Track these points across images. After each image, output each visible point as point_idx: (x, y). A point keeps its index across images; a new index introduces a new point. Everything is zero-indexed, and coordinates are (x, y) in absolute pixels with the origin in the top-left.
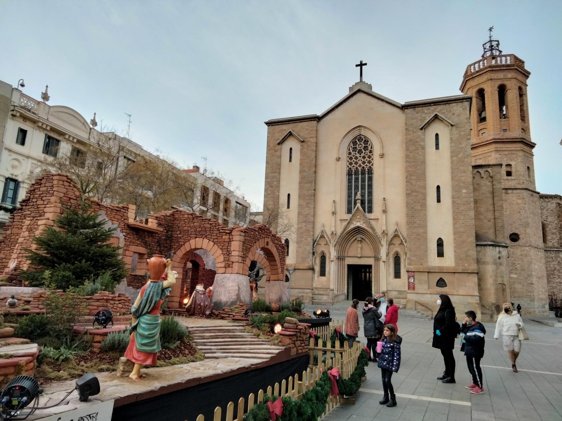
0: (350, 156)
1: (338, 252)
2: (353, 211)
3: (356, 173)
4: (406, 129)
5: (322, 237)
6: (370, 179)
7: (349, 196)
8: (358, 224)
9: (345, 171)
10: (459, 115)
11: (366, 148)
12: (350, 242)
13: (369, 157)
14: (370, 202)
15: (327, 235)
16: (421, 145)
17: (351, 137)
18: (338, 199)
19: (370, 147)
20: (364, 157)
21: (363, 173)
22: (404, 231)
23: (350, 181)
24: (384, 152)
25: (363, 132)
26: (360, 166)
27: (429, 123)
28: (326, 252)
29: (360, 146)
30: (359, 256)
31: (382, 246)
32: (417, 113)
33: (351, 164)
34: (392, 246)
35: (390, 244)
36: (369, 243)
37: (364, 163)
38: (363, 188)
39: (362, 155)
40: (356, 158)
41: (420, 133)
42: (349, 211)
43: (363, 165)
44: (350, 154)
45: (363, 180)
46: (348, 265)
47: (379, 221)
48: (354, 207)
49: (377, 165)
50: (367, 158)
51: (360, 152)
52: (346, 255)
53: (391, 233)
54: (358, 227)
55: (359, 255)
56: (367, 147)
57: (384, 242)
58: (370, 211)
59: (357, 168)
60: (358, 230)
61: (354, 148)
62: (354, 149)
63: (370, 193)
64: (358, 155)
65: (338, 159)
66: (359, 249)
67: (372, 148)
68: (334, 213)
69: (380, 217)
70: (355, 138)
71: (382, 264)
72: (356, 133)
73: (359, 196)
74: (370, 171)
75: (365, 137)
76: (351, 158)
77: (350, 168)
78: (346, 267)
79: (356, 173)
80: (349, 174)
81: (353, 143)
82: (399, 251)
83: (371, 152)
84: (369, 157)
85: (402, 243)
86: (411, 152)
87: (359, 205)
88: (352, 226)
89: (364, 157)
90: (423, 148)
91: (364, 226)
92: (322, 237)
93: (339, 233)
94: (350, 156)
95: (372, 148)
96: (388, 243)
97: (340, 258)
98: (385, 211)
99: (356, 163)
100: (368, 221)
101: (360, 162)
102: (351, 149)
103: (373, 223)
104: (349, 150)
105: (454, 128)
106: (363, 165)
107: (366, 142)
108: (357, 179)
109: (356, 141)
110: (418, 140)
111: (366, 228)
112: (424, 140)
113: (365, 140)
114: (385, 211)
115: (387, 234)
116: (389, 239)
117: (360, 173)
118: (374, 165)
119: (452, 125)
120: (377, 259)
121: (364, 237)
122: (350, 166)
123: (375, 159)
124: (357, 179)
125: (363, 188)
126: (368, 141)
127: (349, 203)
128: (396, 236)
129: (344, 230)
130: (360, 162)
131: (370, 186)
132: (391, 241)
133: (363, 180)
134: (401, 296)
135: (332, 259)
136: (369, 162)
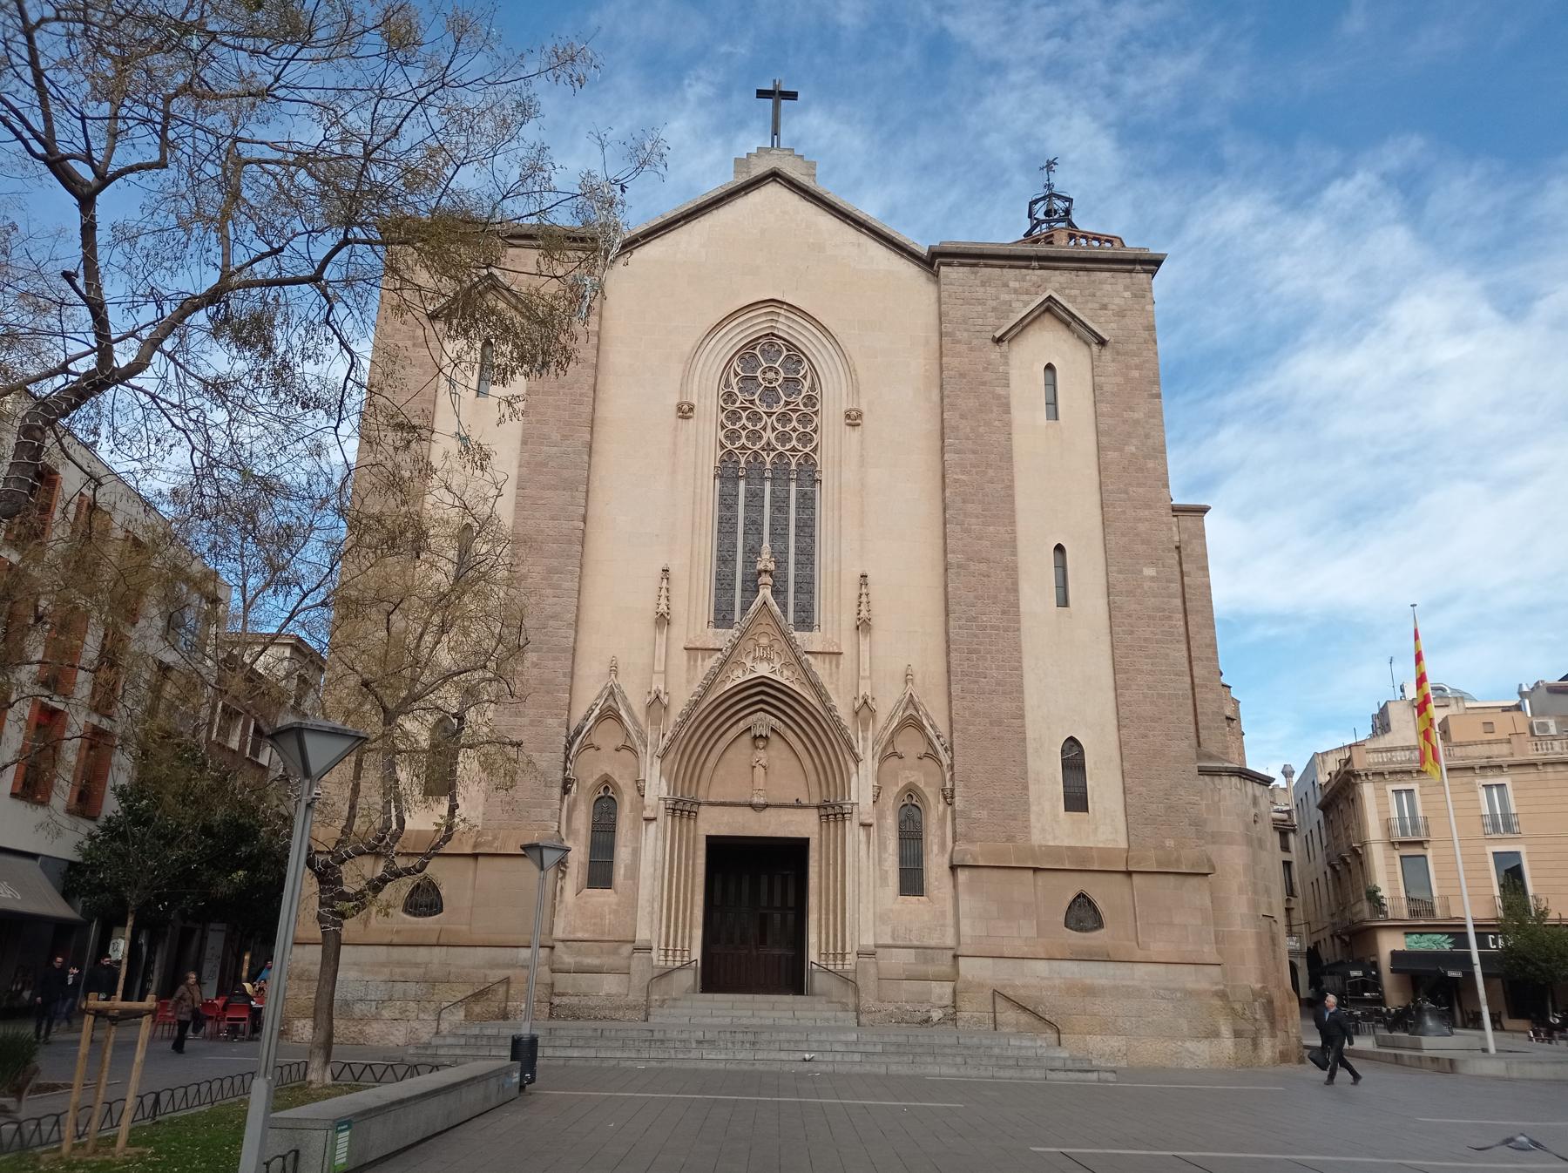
1: (673, 779)
3: (755, 471)
7: (725, 558)
8: (763, 670)
10: (1121, 314)
11: (792, 383)
14: (806, 586)
16: (999, 397)
17: (735, 337)
19: (807, 384)
22: (935, 712)
23: (726, 503)
25: (785, 326)
27: (1023, 325)
29: (771, 375)
31: (857, 760)
32: (983, 284)
33: (732, 436)
34: (894, 761)
35: (889, 753)
38: (779, 533)
39: (778, 409)
40: (755, 417)
41: (995, 353)
42: (722, 618)
44: (730, 398)
45: (780, 505)
46: (708, 837)
47: (846, 662)
51: (770, 394)
53: (887, 707)
54: (763, 682)
55: (760, 793)
57: (866, 747)
58: (806, 620)
60: (763, 693)
61: (744, 379)
62: (748, 381)
63: (807, 556)
67: (813, 388)
70: (752, 344)
71: (853, 832)
72: (758, 324)
73: (765, 561)
74: (809, 474)
75: (790, 346)
76: (734, 416)
79: (755, 471)
80: (727, 474)
83: (810, 400)
84: (805, 419)
86: (963, 417)
87: (765, 592)
88: (739, 677)
89: (784, 418)
91: (785, 677)
94: (730, 408)
96: (879, 749)
98: (863, 626)
99: (755, 436)
100: (797, 660)
102: (734, 381)
103: (819, 667)
104: (728, 384)
105: (1107, 354)
107: (796, 356)
108: (754, 498)
110: (988, 376)
114: (863, 626)
119: (1102, 342)
120: (833, 812)
124: (754, 498)
125: (779, 533)
127: (723, 584)
128: (913, 722)
129: (707, 689)
130: (769, 435)
131: (807, 528)
132: (891, 741)
133: (780, 505)
134: (931, 969)
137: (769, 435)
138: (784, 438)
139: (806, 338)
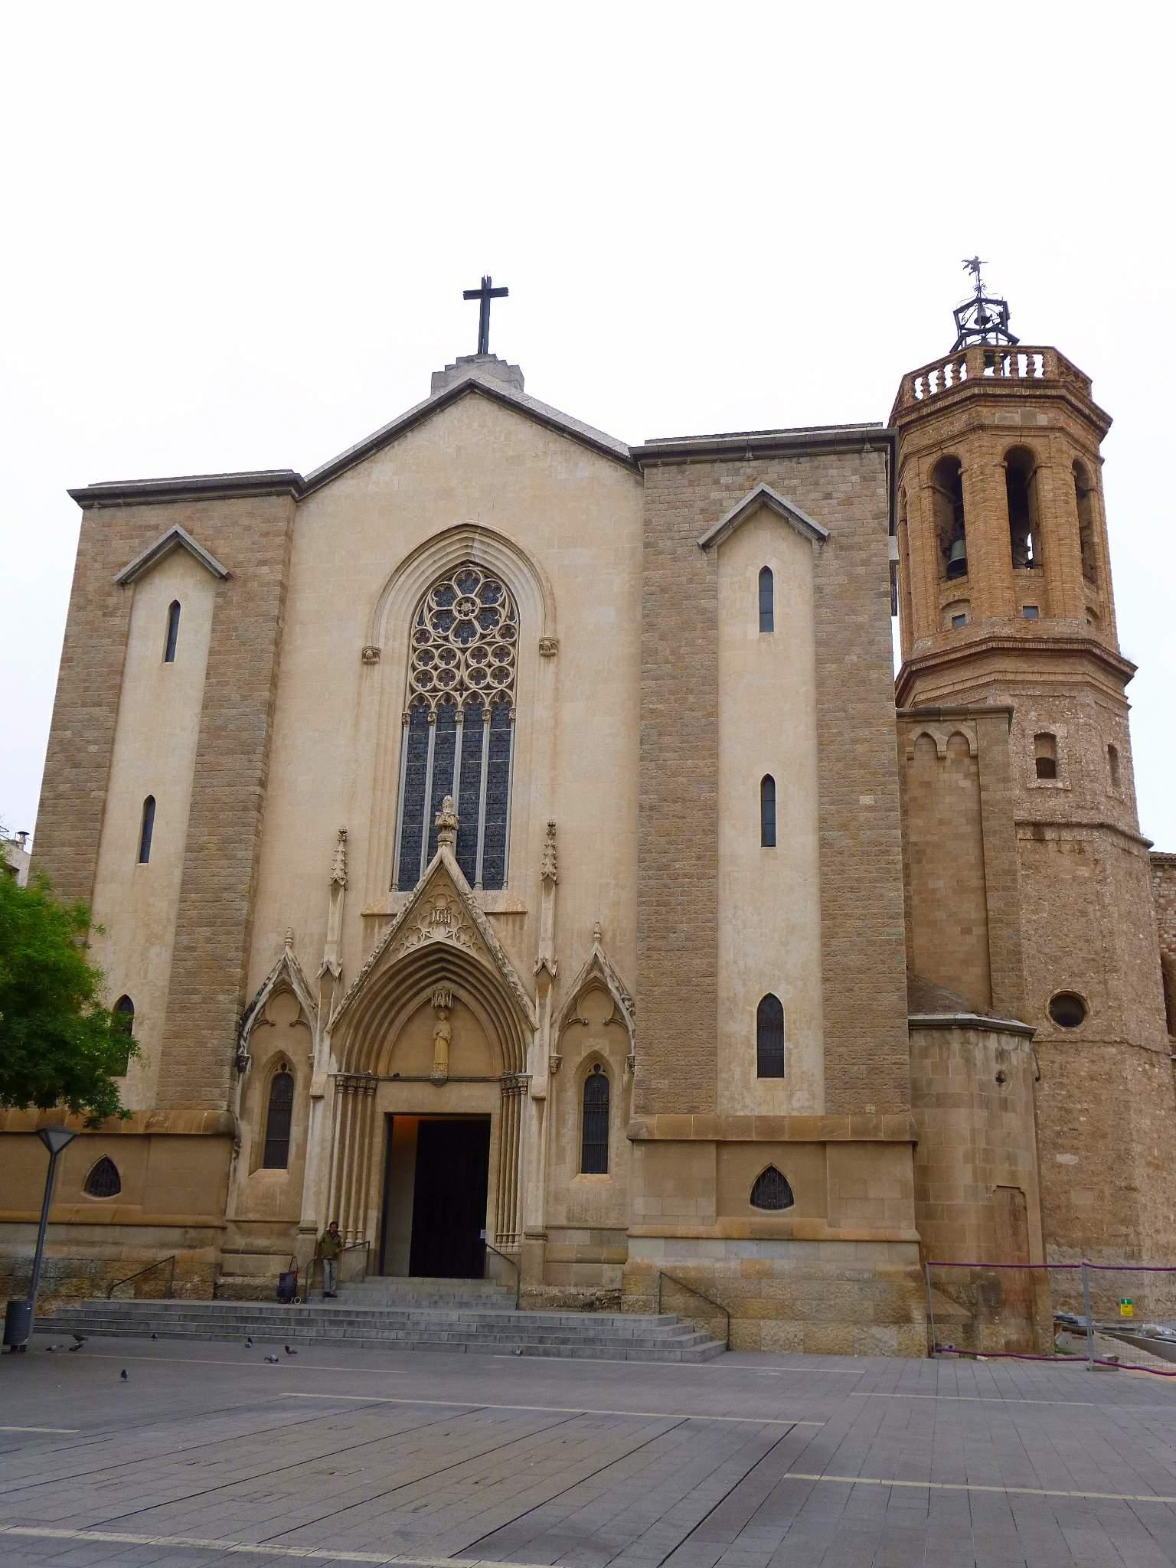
0: (423, 646)
4: (647, 545)
5: (283, 989)
6: (501, 744)
7: (412, 812)
8: (439, 935)
11: (488, 616)
14: (497, 840)
16: (703, 611)
18: (358, 825)
19: (504, 613)
20: (479, 654)
21: (473, 720)
24: (561, 636)
25: (479, 551)
26: (462, 687)
28: (296, 1058)
29: (467, 606)
30: (437, 1075)
38: (470, 781)
39: (473, 643)
41: (701, 562)
44: (423, 636)
47: (527, 920)
48: (429, 861)
49: (533, 685)
50: (490, 658)
51: (464, 630)
55: (438, 1071)
56: (494, 611)
58: (494, 879)
59: (448, 697)
60: (439, 961)
62: (442, 618)
63: (498, 804)
64: (455, 644)
65: (370, 657)
66: (441, 1045)
67: (511, 617)
69: (530, 908)
70: (448, 575)
72: (453, 553)
75: (488, 572)
76: (426, 657)
77: (421, 698)
78: (380, 1122)
80: (416, 718)
81: (437, 593)
82: (606, 1053)
83: (508, 632)
84: (501, 653)
85: (616, 1020)
87: (446, 853)
88: (414, 944)
89: (479, 654)
90: (712, 622)
91: (461, 943)
92: (283, 989)
93: (353, 978)
94: (423, 646)
95: (511, 617)
97: (355, 1086)
98: (550, 882)
101: (462, 674)
104: (421, 622)
107: (493, 587)
108: (445, 743)
109: (449, 588)
111: (473, 953)
112: (713, 591)
113: (486, 585)
114: (550, 882)
115: (554, 979)
116: (565, 1000)
117: (459, 717)
118: (519, 685)
122: (419, 688)
123: (520, 662)
124: (445, 743)
125: (470, 781)
127: (409, 843)
128: (594, 985)
129: (380, 959)
130: (462, 674)
131: (500, 774)
135: (315, 1090)
138: (478, 675)
139: (503, 564)
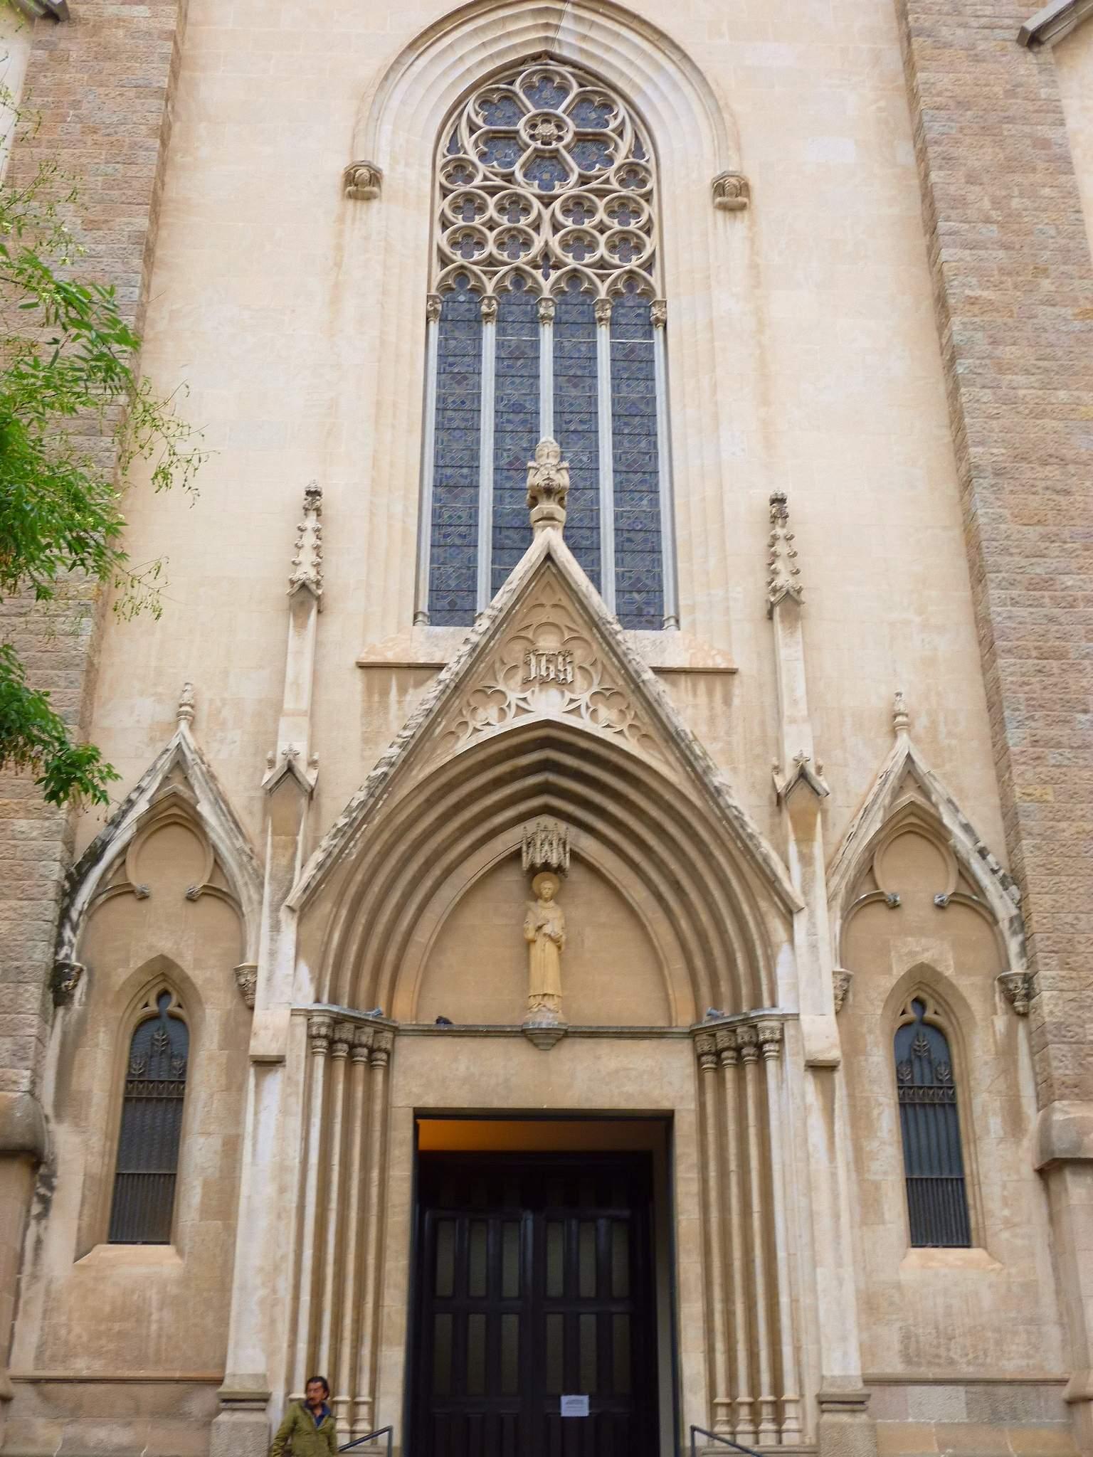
2: (489, 605)
6: (636, 367)
9: (416, 281)
11: (593, 143)
12: (450, 893)
13: (623, 209)
14: (642, 540)
15: (220, 800)
19: (625, 145)
23: (455, 369)
33: (468, 240)
36: (637, 894)
37: (580, 243)
40: (517, 205)
42: (448, 601)
43: (571, 262)
44: (460, 169)
45: (576, 371)
51: (546, 162)
52: (403, 1012)
56: (600, 140)
58: (644, 605)
61: (492, 138)
62: (499, 140)
63: (640, 473)
67: (638, 150)
68: (306, 597)
70: (509, 71)
74: (639, 309)
75: (586, 75)
80: (455, 306)
81: (484, 103)
83: (633, 173)
89: (578, 207)
95: (638, 150)
99: (516, 240)
102: (467, 141)
104: (454, 145)
106: (571, 262)
108: (517, 362)
109: (509, 97)
113: (584, 99)
121: (589, 847)
122: (459, 258)
124: (517, 362)
126: (608, 107)
130: (545, 238)
131: (638, 419)
133: (576, 371)
136: (626, 243)
137: (545, 238)
